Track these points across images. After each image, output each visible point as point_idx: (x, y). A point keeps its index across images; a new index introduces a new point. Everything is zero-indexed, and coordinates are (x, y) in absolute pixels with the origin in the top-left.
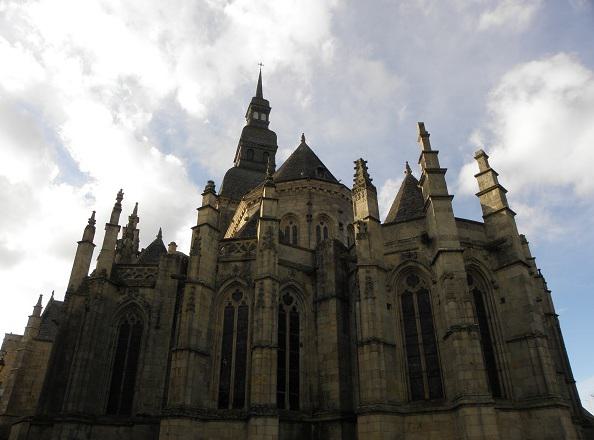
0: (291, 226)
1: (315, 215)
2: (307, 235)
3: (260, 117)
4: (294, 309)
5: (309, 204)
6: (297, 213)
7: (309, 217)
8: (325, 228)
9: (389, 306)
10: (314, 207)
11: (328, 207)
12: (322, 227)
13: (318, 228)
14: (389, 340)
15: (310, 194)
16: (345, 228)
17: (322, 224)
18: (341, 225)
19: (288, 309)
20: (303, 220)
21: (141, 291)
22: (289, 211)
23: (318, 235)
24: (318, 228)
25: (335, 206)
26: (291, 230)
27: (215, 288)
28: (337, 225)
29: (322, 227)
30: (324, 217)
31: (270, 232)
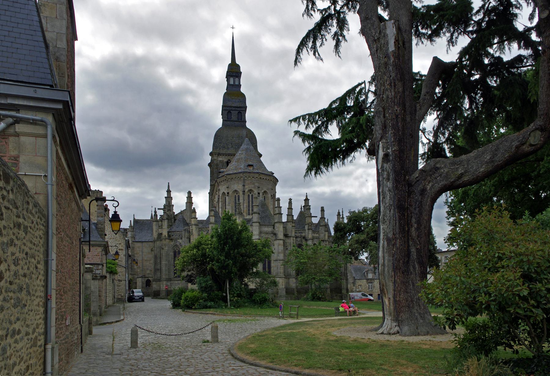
0: (237, 195)
1: (246, 190)
2: (243, 201)
3: (234, 82)
5: (244, 186)
6: (239, 190)
7: (244, 192)
8: (252, 195)
10: (246, 187)
11: (253, 186)
12: (251, 195)
13: (249, 195)
15: (244, 180)
16: (261, 194)
17: (250, 193)
18: (259, 193)
20: (241, 193)
21: (178, 240)
22: (235, 189)
23: (249, 199)
24: (249, 195)
25: (257, 184)
26: (237, 197)
29: (251, 195)
30: (250, 191)
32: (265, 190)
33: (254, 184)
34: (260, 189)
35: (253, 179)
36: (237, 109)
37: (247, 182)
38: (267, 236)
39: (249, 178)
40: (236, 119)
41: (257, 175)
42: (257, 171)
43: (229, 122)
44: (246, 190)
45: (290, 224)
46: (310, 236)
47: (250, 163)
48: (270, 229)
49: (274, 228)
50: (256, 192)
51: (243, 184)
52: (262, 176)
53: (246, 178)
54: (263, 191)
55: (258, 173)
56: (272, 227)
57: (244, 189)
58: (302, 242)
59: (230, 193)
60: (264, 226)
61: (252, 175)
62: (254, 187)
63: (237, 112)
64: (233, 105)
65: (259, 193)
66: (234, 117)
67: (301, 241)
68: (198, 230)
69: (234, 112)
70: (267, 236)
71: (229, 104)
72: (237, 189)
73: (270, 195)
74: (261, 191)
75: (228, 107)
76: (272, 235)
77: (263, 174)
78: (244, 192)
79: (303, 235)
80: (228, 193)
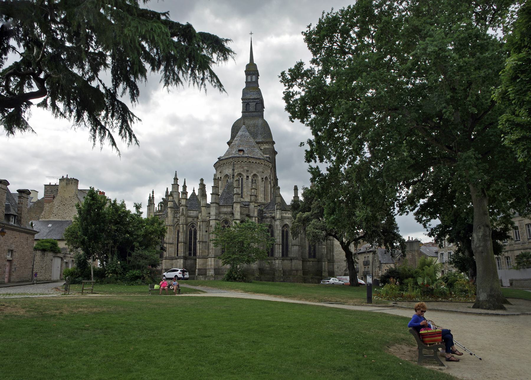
1: (236, 174)
4: (195, 229)
5: (233, 170)
9: (206, 231)
10: (235, 171)
11: (242, 170)
12: (240, 179)
14: (205, 240)
16: (250, 177)
17: (240, 177)
18: (248, 177)
19: (193, 229)
25: (246, 168)
27: (174, 226)
28: (245, 177)
30: (240, 175)
31: (183, 210)
32: (255, 173)
33: (243, 168)
34: (249, 172)
35: (242, 163)
36: (255, 101)
37: (236, 166)
38: (226, 216)
39: (239, 163)
40: (254, 110)
41: (245, 160)
42: (246, 155)
43: (247, 113)
44: (236, 174)
45: (253, 204)
46: (278, 216)
47: (241, 148)
48: (229, 210)
49: (233, 208)
50: (245, 175)
51: (232, 168)
52: (251, 160)
53: (235, 163)
54: (252, 174)
55: (246, 157)
56: (232, 207)
57: (233, 173)
58: (272, 223)
59: (222, 178)
60: (223, 207)
61: (241, 159)
62: (243, 171)
63: (255, 103)
64: (252, 97)
65: (248, 177)
66: (252, 108)
67: (271, 221)
68: (173, 212)
69: (252, 103)
70: (226, 216)
71: (248, 96)
72: (228, 174)
73: (260, 178)
74: (250, 174)
75: (247, 99)
76: (231, 215)
77: (251, 157)
78: (233, 175)
79: (273, 215)
80: (221, 178)
